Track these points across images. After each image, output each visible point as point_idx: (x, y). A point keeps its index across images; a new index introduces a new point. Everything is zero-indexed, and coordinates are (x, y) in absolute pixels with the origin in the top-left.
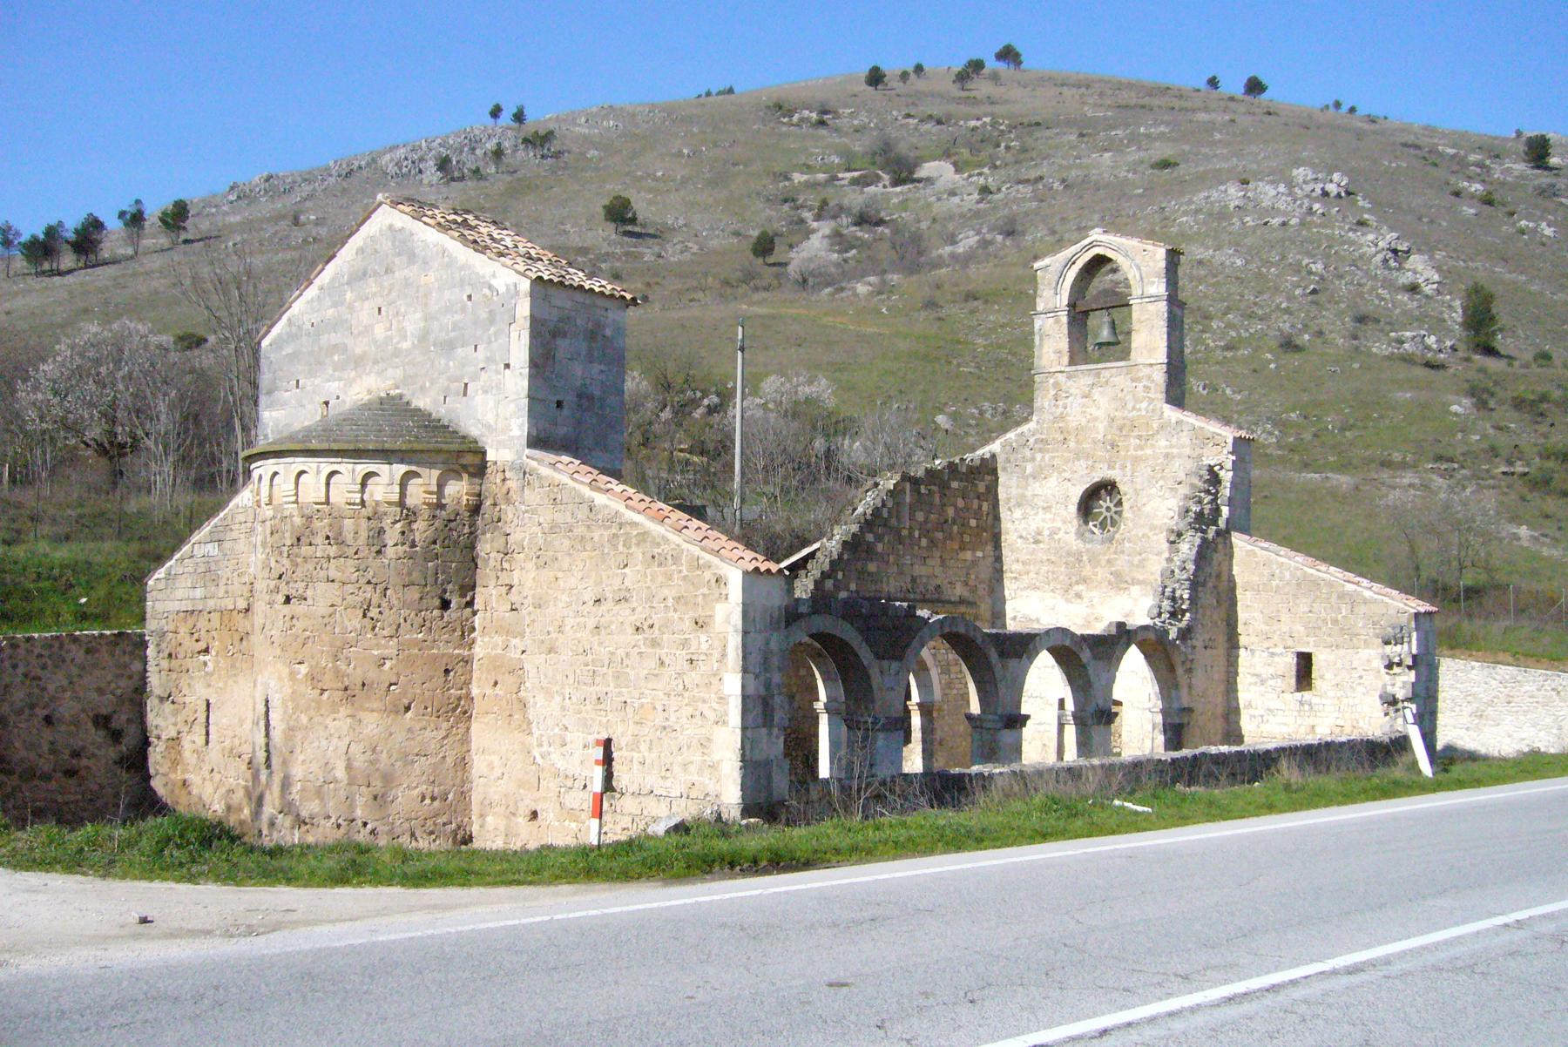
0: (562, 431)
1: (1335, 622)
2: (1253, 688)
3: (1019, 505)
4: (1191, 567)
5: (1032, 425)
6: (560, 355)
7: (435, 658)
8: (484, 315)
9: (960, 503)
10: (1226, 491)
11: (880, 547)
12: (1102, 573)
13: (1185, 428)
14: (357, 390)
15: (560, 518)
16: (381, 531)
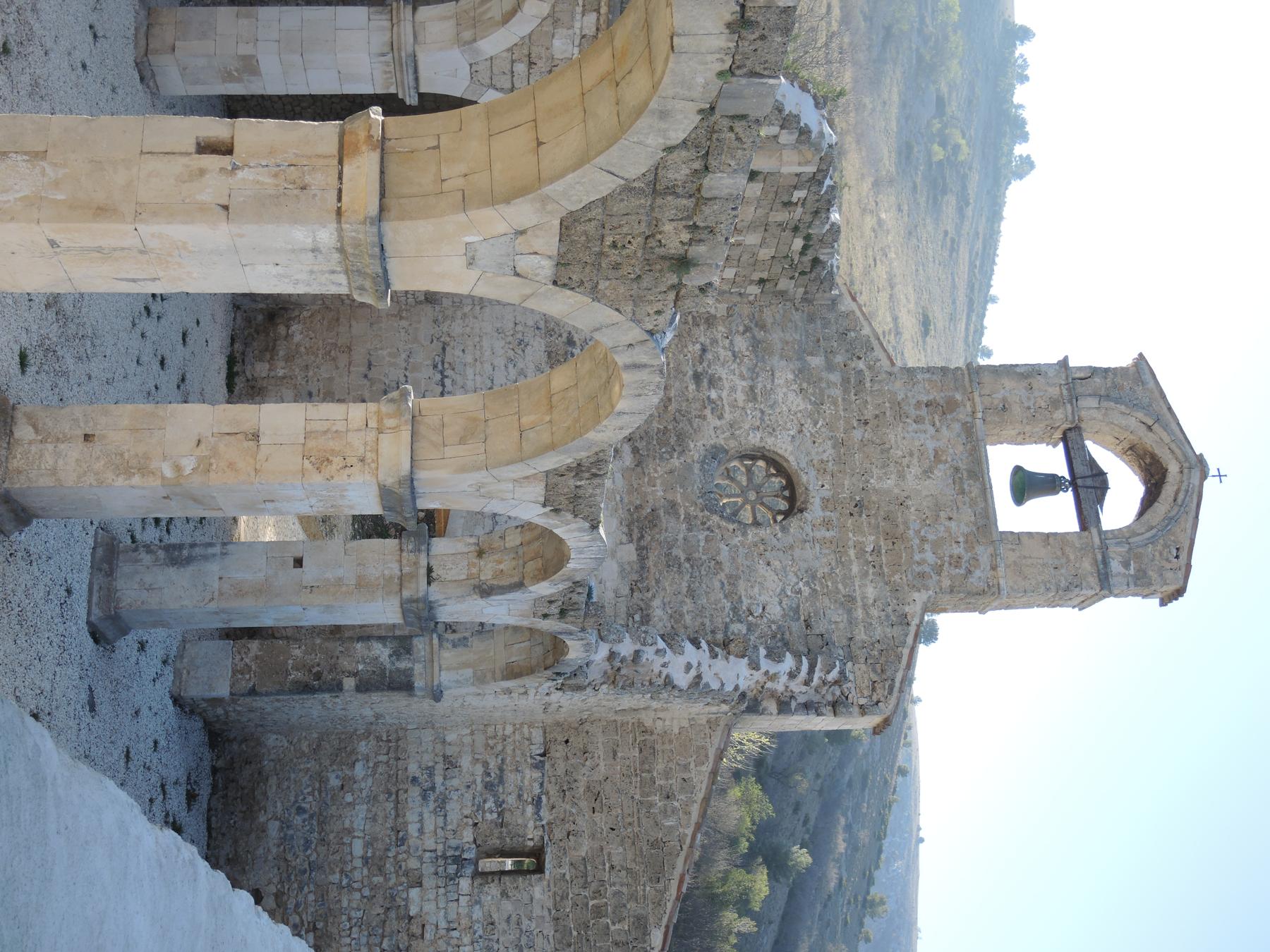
1: (598, 912)
2: (479, 769)
3: (755, 345)
13: (897, 631)
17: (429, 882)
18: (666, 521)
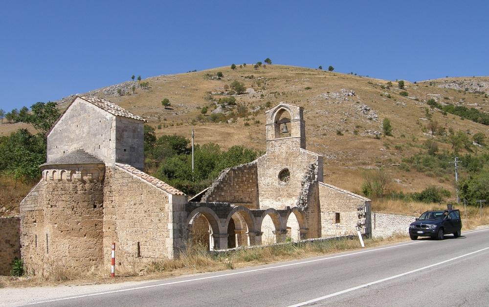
0: (126, 157)
4: (308, 192)
5: (266, 154)
6: (125, 137)
7: (92, 221)
8: (104, 126)
9: (247, 176)
10: (316, 171)
11: (225, 188)
12: (285, 193)
14: (72, 148)
15: (124, 181)
16: (76, 187)
17: (340, 231)
18: (289, 191)
